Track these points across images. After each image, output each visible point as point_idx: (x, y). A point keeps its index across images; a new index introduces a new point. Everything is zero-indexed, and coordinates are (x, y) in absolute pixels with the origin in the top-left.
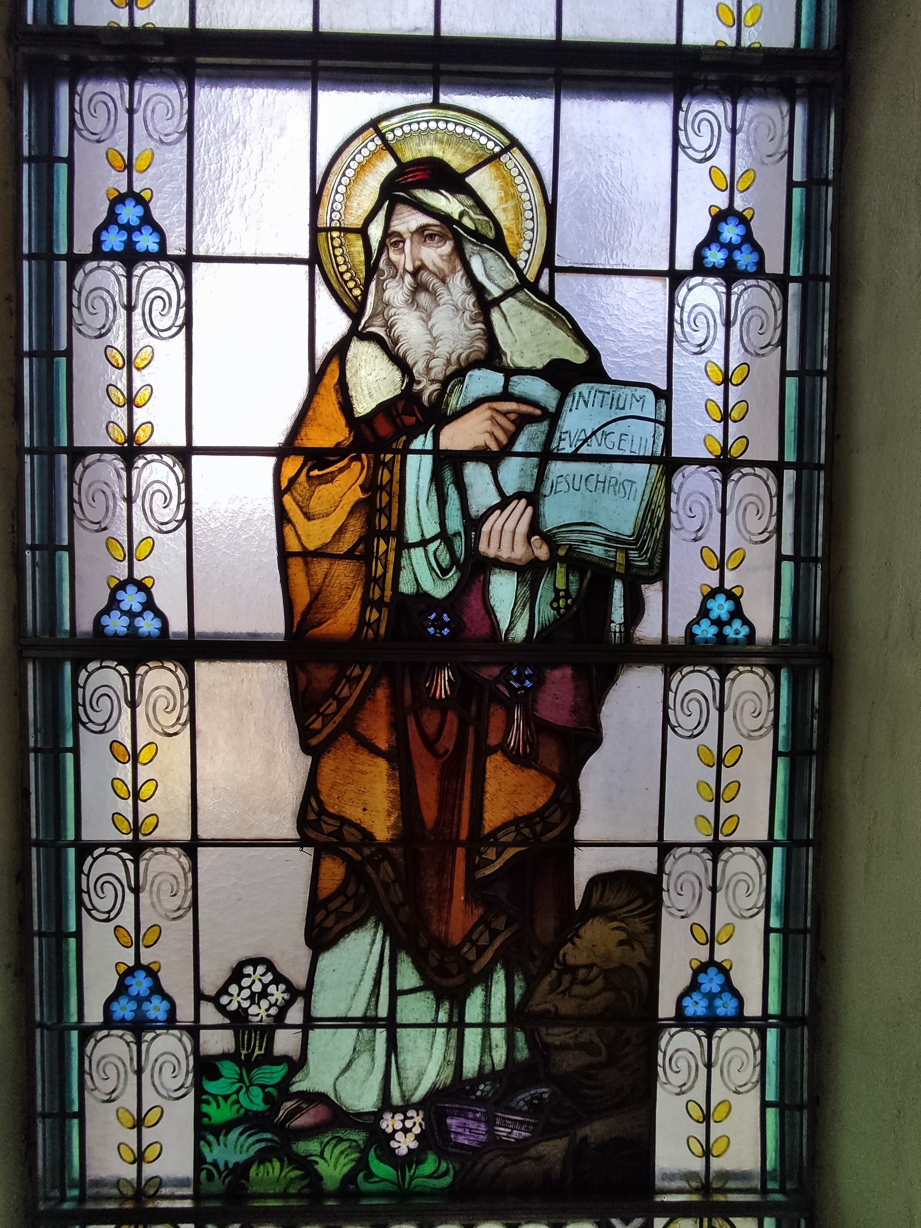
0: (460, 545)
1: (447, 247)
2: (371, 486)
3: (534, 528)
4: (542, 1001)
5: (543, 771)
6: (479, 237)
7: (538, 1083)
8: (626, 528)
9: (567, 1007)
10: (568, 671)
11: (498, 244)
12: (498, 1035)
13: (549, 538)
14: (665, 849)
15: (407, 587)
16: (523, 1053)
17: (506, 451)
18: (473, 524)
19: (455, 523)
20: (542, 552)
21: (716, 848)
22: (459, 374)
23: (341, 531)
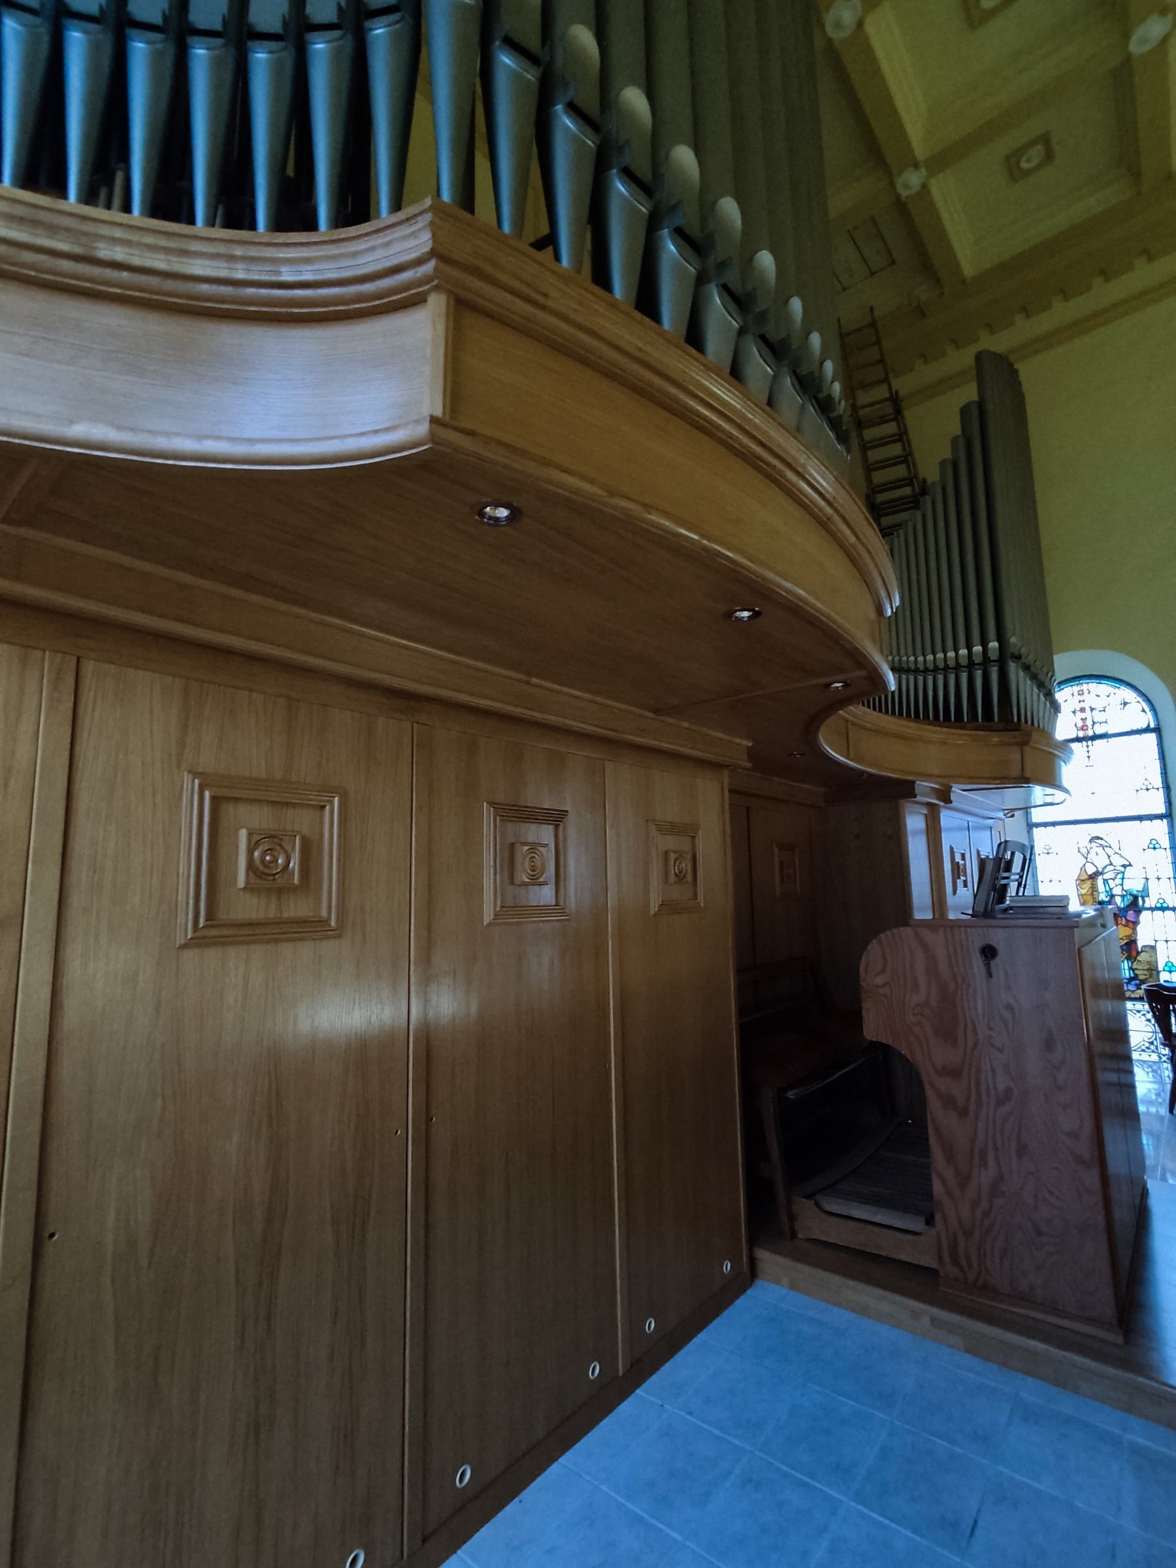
0: (1109, 893)
1: (1101, 848)
2: (1093, 884)
3: (1123, 889)
4: (1135, 966)
5: (1130, 928)
6: (1107, 846)
7: (1136, 980)
8: (1141, 889)
9: (1140, 968)
10: (1132, 912)
11: (1110, 847)
12: (1127, 972)
13: (1125, 891)
14: (1156, 941)
15: (1100, 899)
16: (1132, 975)
17: (1116, 878)
18: (1111, 889)
19: (1108, 889)
20: (1124, 893)
21: (1167, 941)
22: (1105, 867)
23: (1088, 891)
